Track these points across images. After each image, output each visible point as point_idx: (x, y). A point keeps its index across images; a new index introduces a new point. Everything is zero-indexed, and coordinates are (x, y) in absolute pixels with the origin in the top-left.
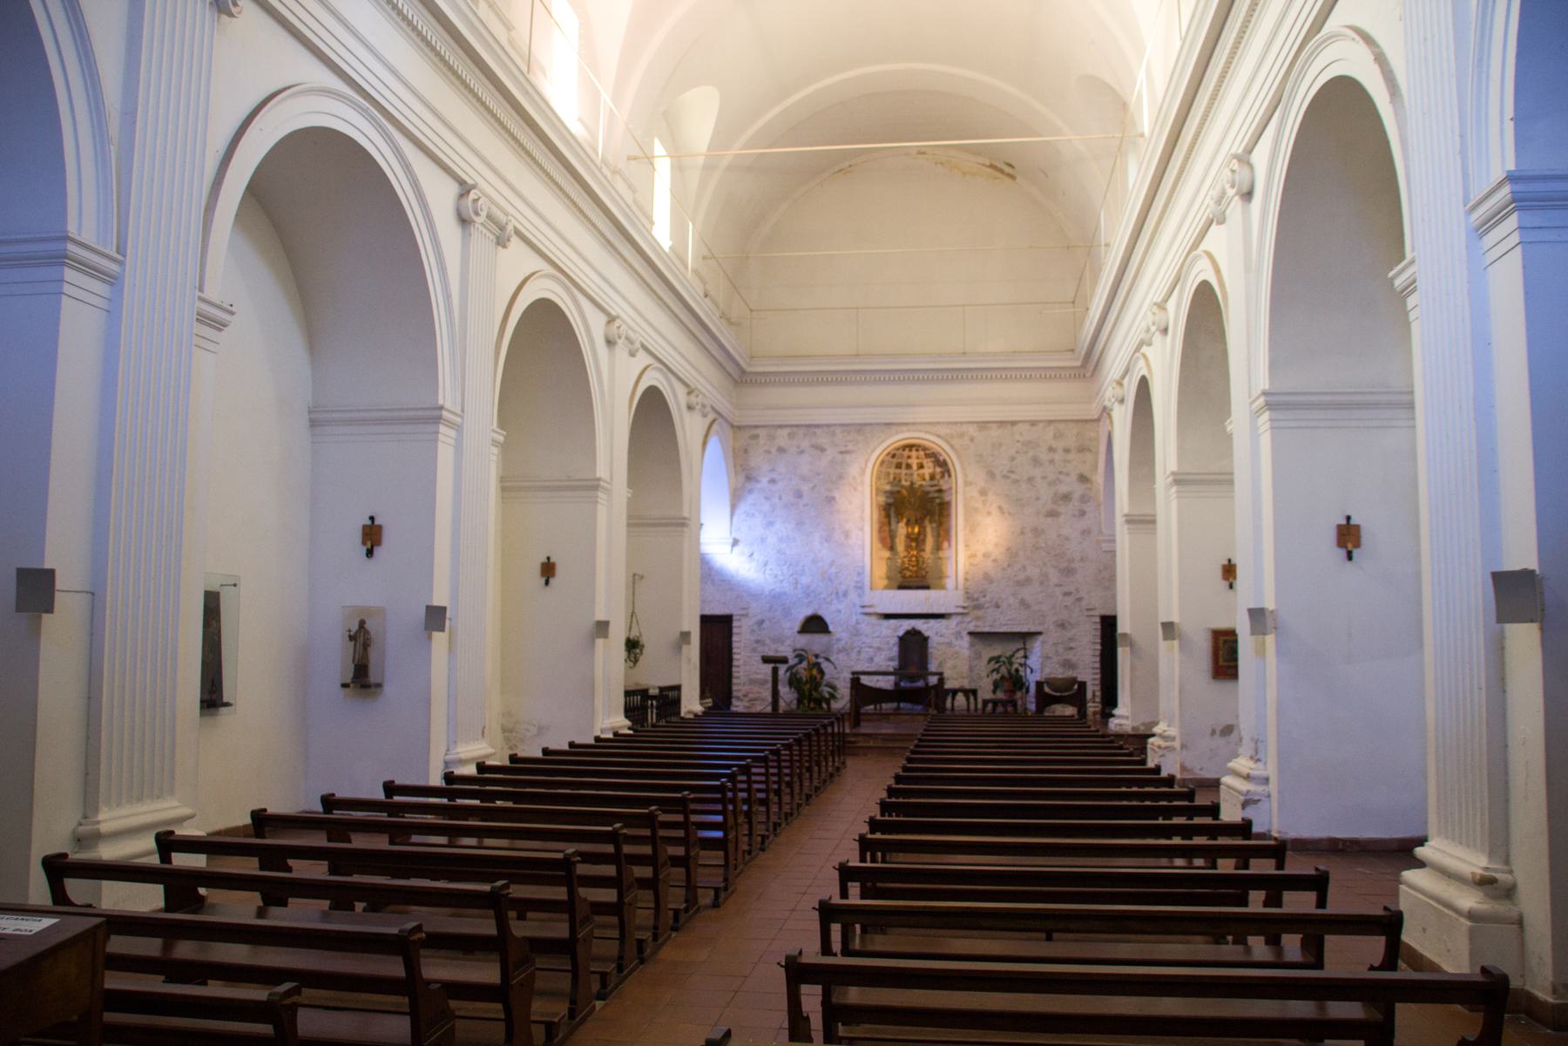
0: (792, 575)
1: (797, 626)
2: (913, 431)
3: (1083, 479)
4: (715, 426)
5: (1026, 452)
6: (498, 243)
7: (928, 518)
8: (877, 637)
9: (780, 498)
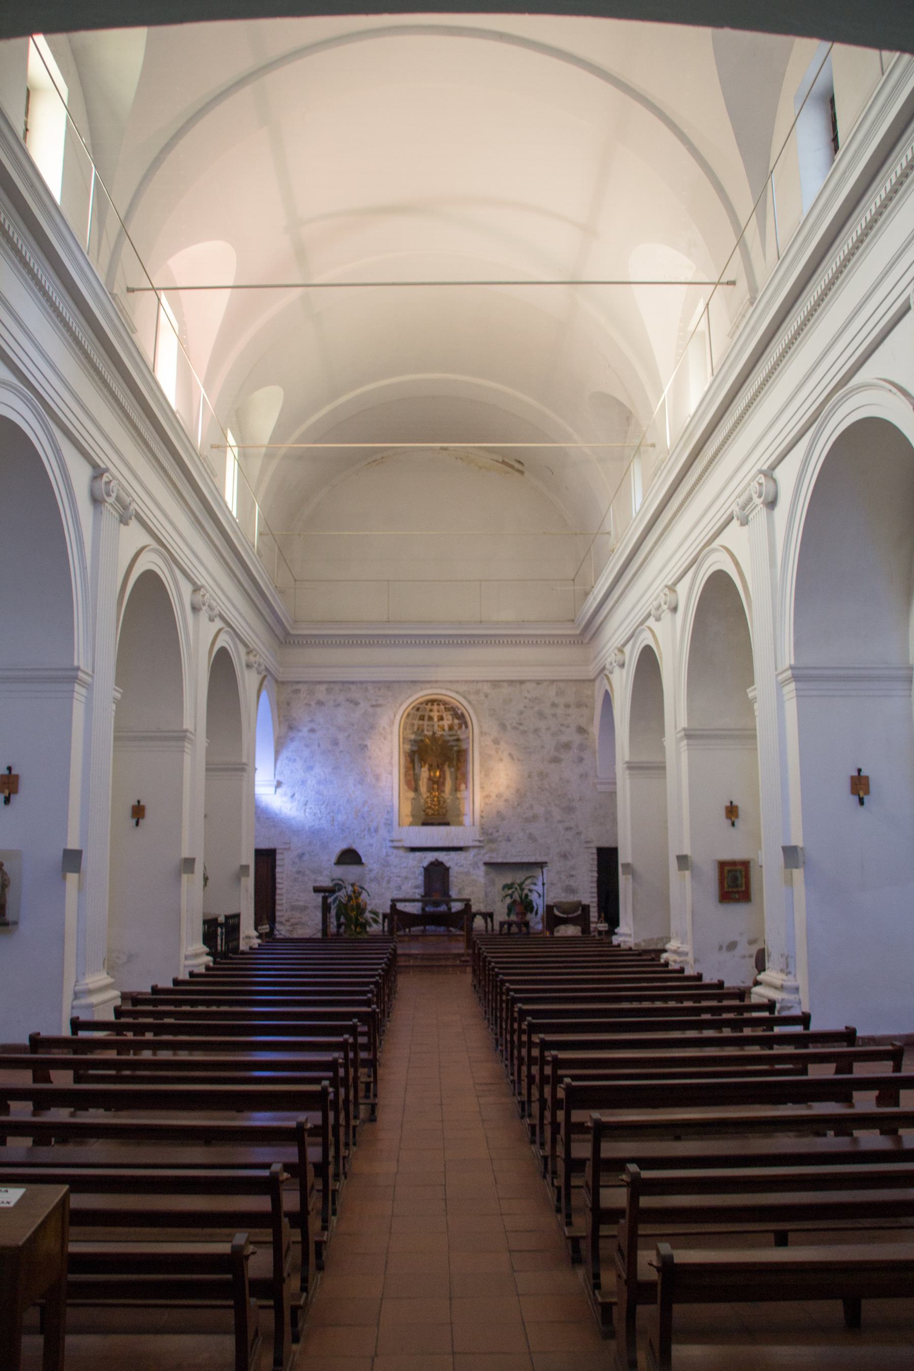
0: (329, 813)
1: (334, 859)
2: (436, 688)
3: (581, 730)
4: (266, 683)
5: (532, 708)
6: (121, 521)
7: (447, 763)
8: (406, 867)
9: (319, 746)
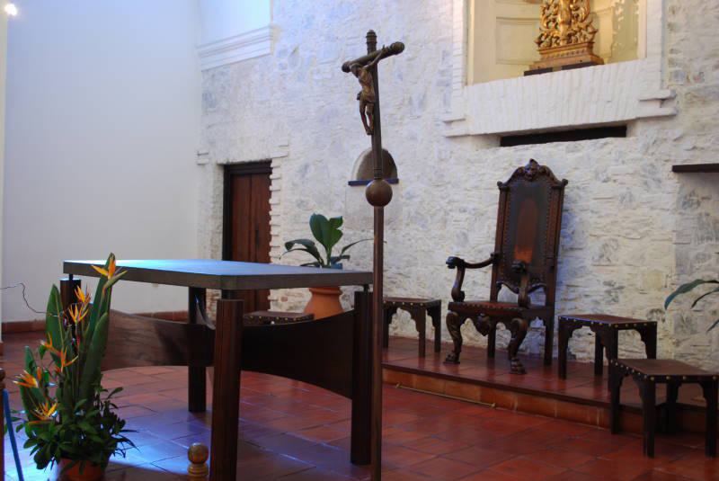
8: (476, 187)
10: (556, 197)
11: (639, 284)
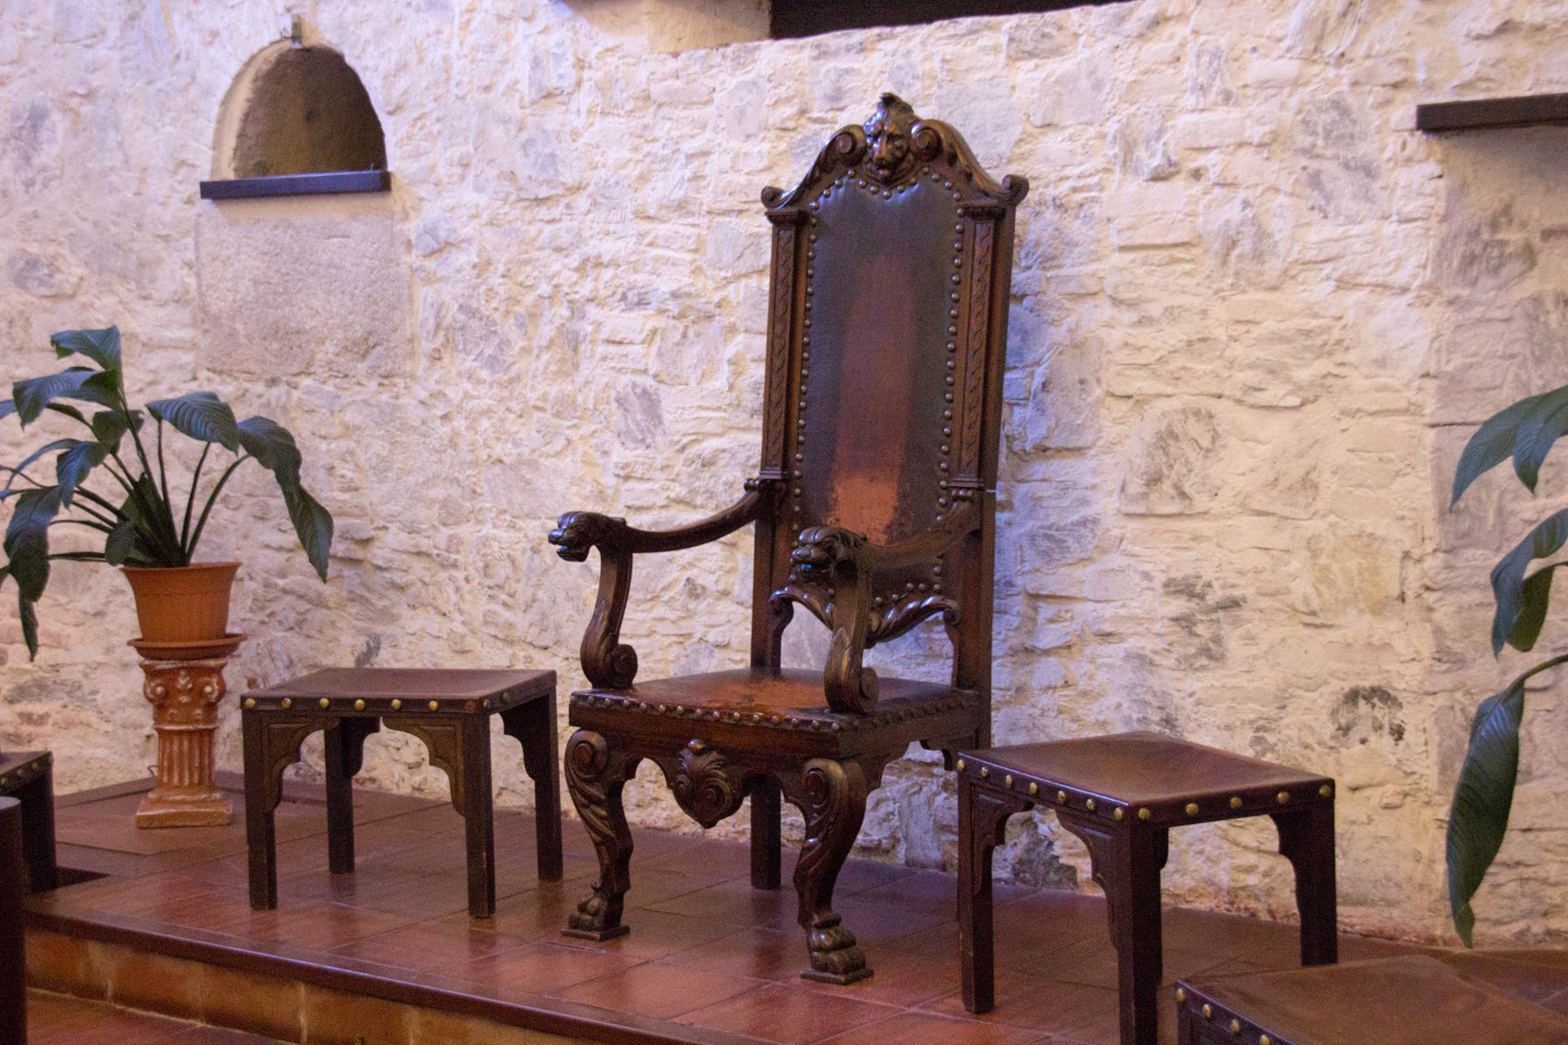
8: (681, 207)
10: (981, 249)
11: (1302, 588)
